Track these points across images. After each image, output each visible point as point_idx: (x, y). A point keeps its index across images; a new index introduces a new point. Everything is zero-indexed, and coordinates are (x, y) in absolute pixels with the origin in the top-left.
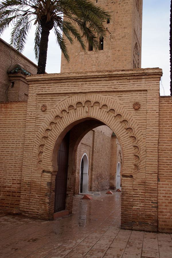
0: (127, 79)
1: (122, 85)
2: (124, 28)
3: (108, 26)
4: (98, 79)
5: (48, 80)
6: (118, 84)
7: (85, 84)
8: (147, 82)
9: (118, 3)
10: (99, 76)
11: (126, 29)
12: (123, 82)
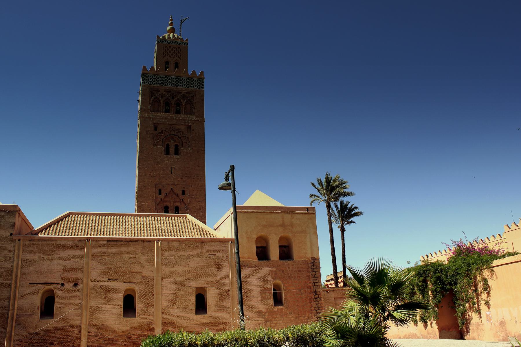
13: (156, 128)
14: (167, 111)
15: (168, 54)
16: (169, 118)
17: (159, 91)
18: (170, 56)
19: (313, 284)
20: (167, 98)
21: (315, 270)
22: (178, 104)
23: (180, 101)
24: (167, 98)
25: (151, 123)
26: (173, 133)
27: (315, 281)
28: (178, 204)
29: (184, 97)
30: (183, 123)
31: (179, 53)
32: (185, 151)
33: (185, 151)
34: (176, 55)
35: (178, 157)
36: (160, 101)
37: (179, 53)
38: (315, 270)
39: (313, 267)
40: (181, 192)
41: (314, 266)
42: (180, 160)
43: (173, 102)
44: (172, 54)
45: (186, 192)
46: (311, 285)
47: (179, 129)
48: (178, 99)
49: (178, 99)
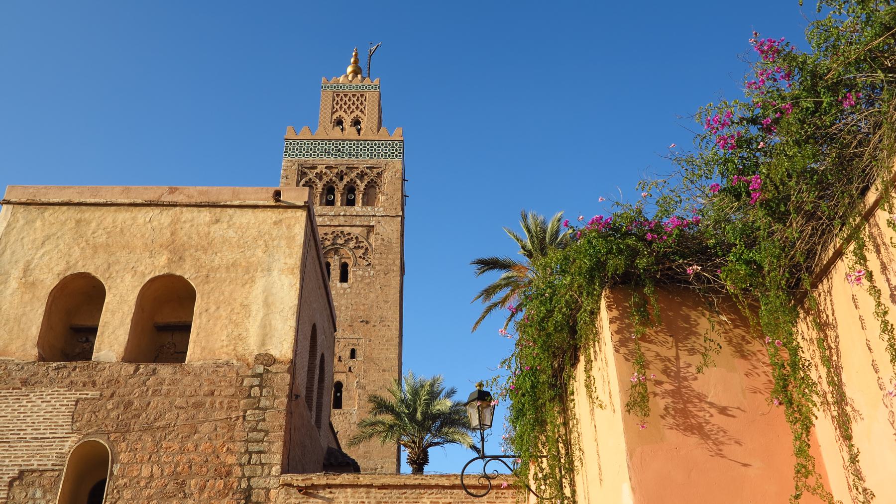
2: (384, 371)
9: (373, 323)
11: (386, 373)
14: (331, 203)
15: (341, 108)
16: (333, 213)
17: (316, 168)
18: (345, 111)
19: (245, 459)
20: (331, 180)
21: (264, 403)
22: (351, 189)
23: (355, 182)
24: (331, 180)
27: (254, 447)
30: (358, 223)
31: (362, 104)
32: (361, 273)
33: (361, 273)
34: (357, 108)
35: (345, 285)
37: (362, 104)
38: (264, 403)
39: (256, 391)
40: (348, 353)
41: (261, 386)
42: (349, 290)
44: (349, 108)
45: (359, 353)
46: (231, 460)
47: (349, 234)
48: (351, 180)
49: (351, 180)
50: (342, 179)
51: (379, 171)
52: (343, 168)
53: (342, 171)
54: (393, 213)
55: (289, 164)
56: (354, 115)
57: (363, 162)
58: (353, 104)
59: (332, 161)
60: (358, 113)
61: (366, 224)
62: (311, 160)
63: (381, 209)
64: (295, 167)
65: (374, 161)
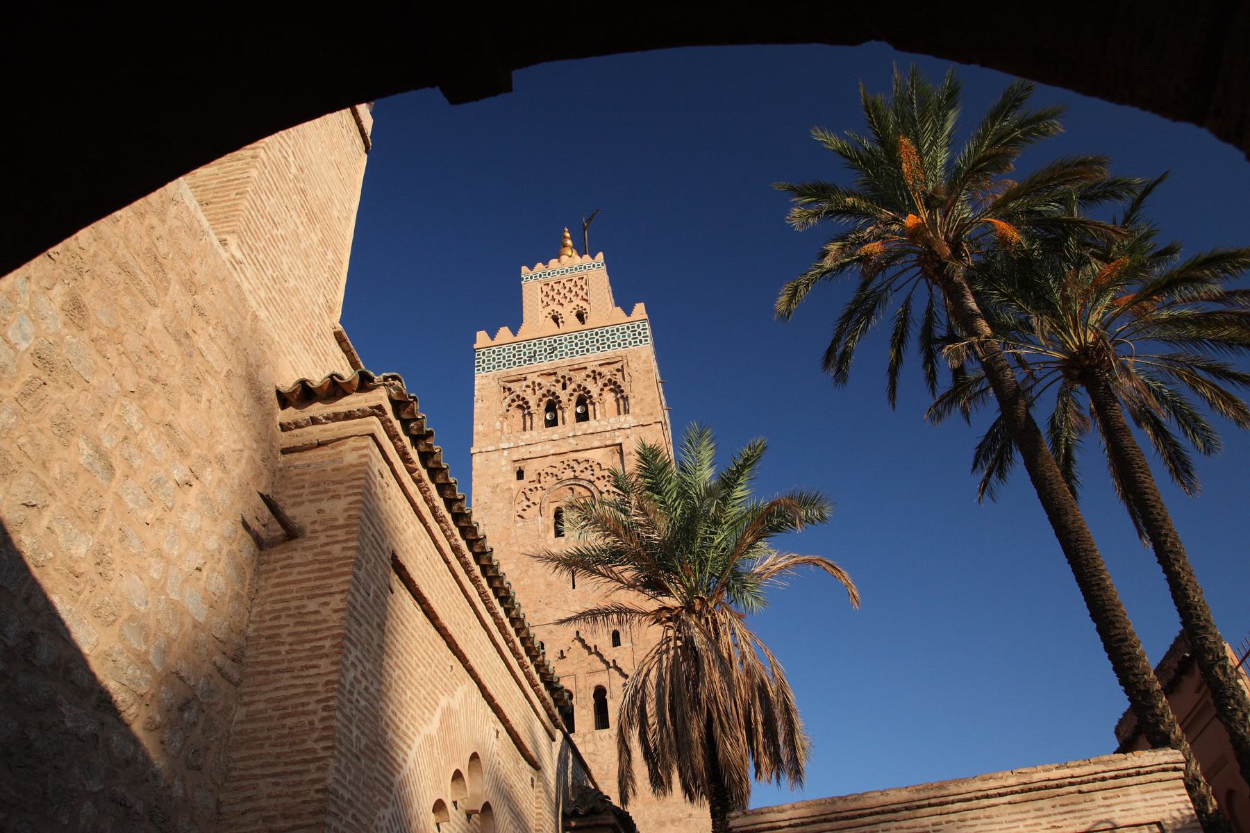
0: (1080, 792)
1: (1072, 815)
3: (616, 654)
4: (985, 802)
5: (814, 822)
6: (1056, 811)
7: (947, 822)
8: (1148, 796)
10: (990, 792)
12: (1073, 804)
13: (520, 474)
14: (552, 423)
22: (583, 400)
25: (504, 462)
26: (569, 474)
28: (602, 679)
29: (595, 376)
30: (596, 444)
36: (527, 403)
43: (563, 396)
48: (579, 386)
49: (579, 386)
50: (564, 387)
51: (618, 366)
52: (565, 372)
53: (563, 377)
54: (650, 420)
55: (484, 381)
56: (574, 305)
57: (592, 359)
58: (570, 291)
59: (546, 365)
60: (577, 301)
61: (609, 442)
62: (514, 371)
63: (629, 417)
64: (494, 384)
65: (610, 353)
